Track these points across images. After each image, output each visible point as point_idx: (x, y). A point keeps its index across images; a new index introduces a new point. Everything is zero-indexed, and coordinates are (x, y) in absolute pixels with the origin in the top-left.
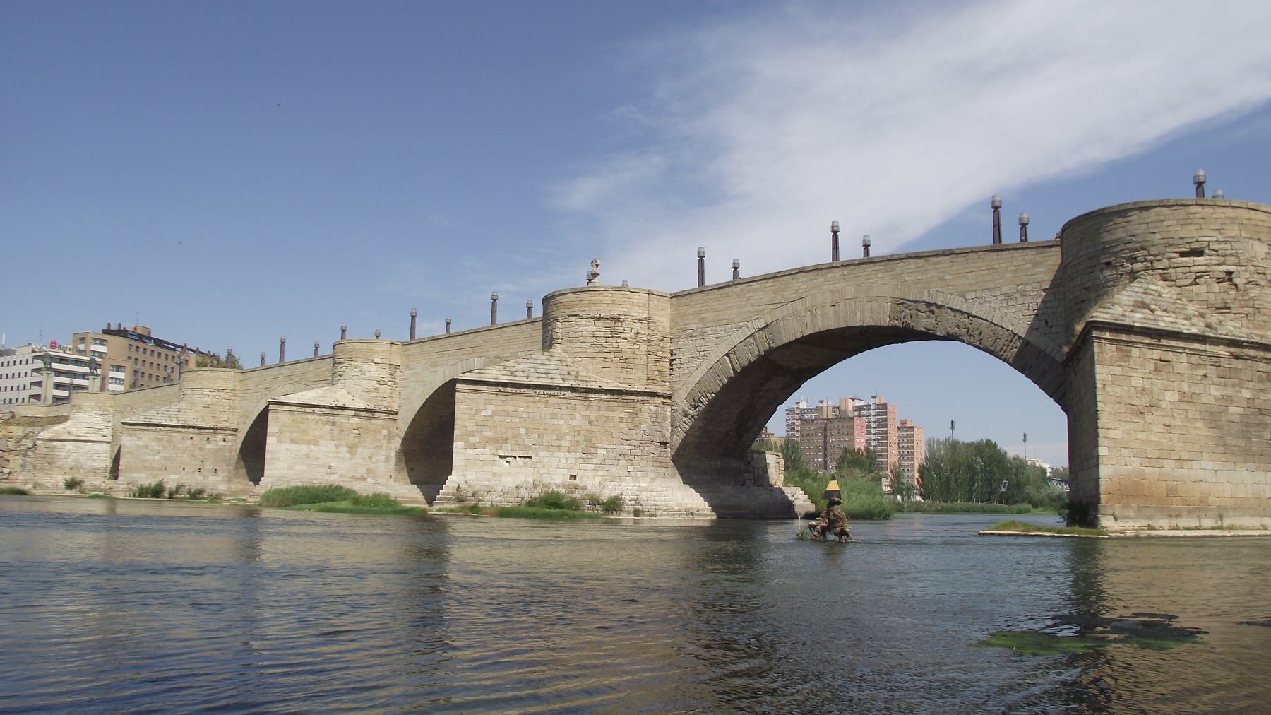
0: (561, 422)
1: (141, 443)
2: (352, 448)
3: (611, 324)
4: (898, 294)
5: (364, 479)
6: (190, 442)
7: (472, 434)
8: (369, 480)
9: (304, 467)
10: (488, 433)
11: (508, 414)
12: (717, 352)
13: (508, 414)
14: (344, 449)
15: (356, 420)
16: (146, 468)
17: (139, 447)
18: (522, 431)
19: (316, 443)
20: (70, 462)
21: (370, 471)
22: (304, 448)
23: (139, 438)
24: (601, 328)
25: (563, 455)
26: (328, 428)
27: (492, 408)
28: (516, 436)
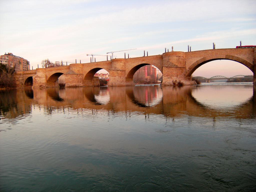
0: (174, 72)
1: (68, 78)
2: (120, 77)
3: (179, 57)
4: (227, 54)
5: (122, 82)
6: (76, 77)
7: (165, 75)
8: (123, 82)
9: (114, 81)
10: (167, 74)
11: (168, 71)
12: (196, 61)
13: (168, 71)
14: (119, 77)
15: (120, 72)
16: (70, 82)
17: (68, 78)
18: (170, 74)
19: (115, 77)
20: (39, 82)
21: (123, 81)
22: (114, 77)
23: (68, 77)
24: (177, 58)
25: (175, 77)
26: (117, 74)
27: (167, 71)
28: (170, 75)
